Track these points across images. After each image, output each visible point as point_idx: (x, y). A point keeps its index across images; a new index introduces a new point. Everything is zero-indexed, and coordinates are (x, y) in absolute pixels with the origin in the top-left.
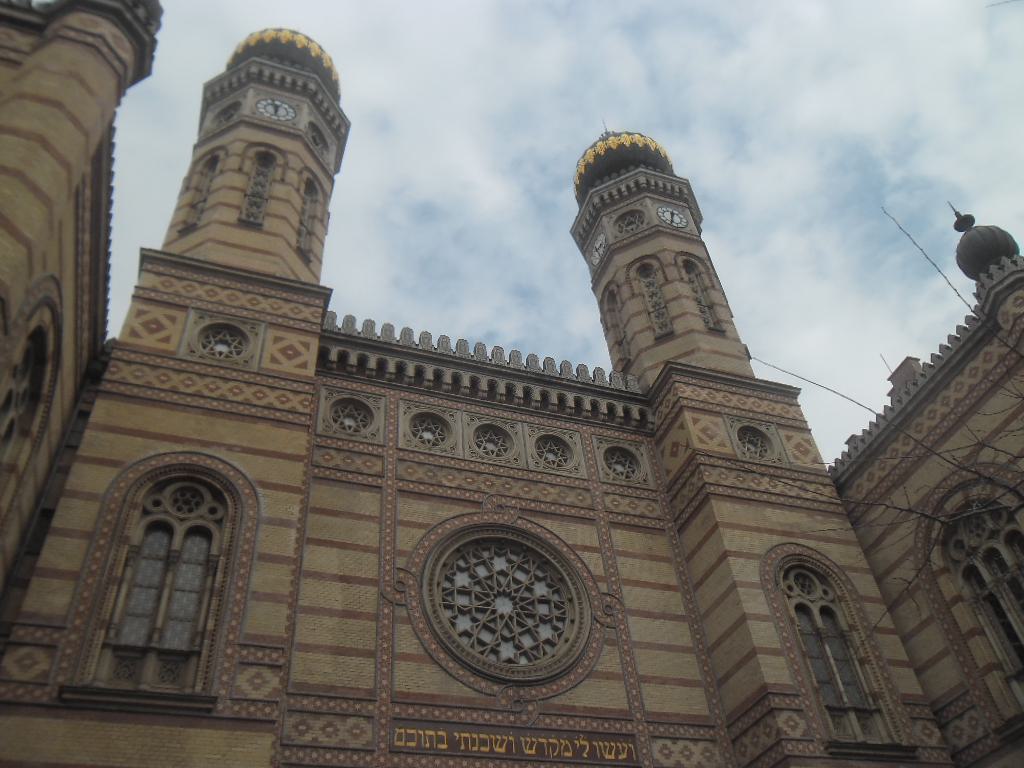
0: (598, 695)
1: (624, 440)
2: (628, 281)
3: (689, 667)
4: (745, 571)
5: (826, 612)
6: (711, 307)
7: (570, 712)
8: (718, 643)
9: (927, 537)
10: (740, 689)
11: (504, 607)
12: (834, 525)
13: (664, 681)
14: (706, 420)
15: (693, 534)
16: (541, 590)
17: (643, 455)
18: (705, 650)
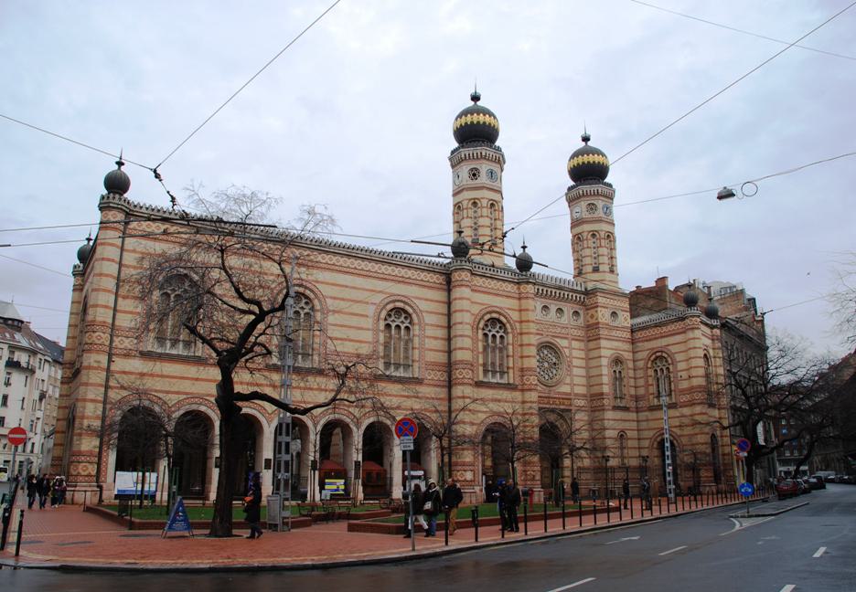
0: (565, 389)
1: (577, 308)
2: (587, 239)
3: (583, 381)
4: (604, 362)
5: (620, 372)
6: (612, 258)
7: (559, 393)
8: (593, 376)
9: (649, 359)
10: (596, 390)
11: (546, 365)
12: (627, 346)
13: (578, 385)
14: (603, 309)
15: (592, 345)
16: (554, 360)
17: (581, 312)
18: (589, 377)
